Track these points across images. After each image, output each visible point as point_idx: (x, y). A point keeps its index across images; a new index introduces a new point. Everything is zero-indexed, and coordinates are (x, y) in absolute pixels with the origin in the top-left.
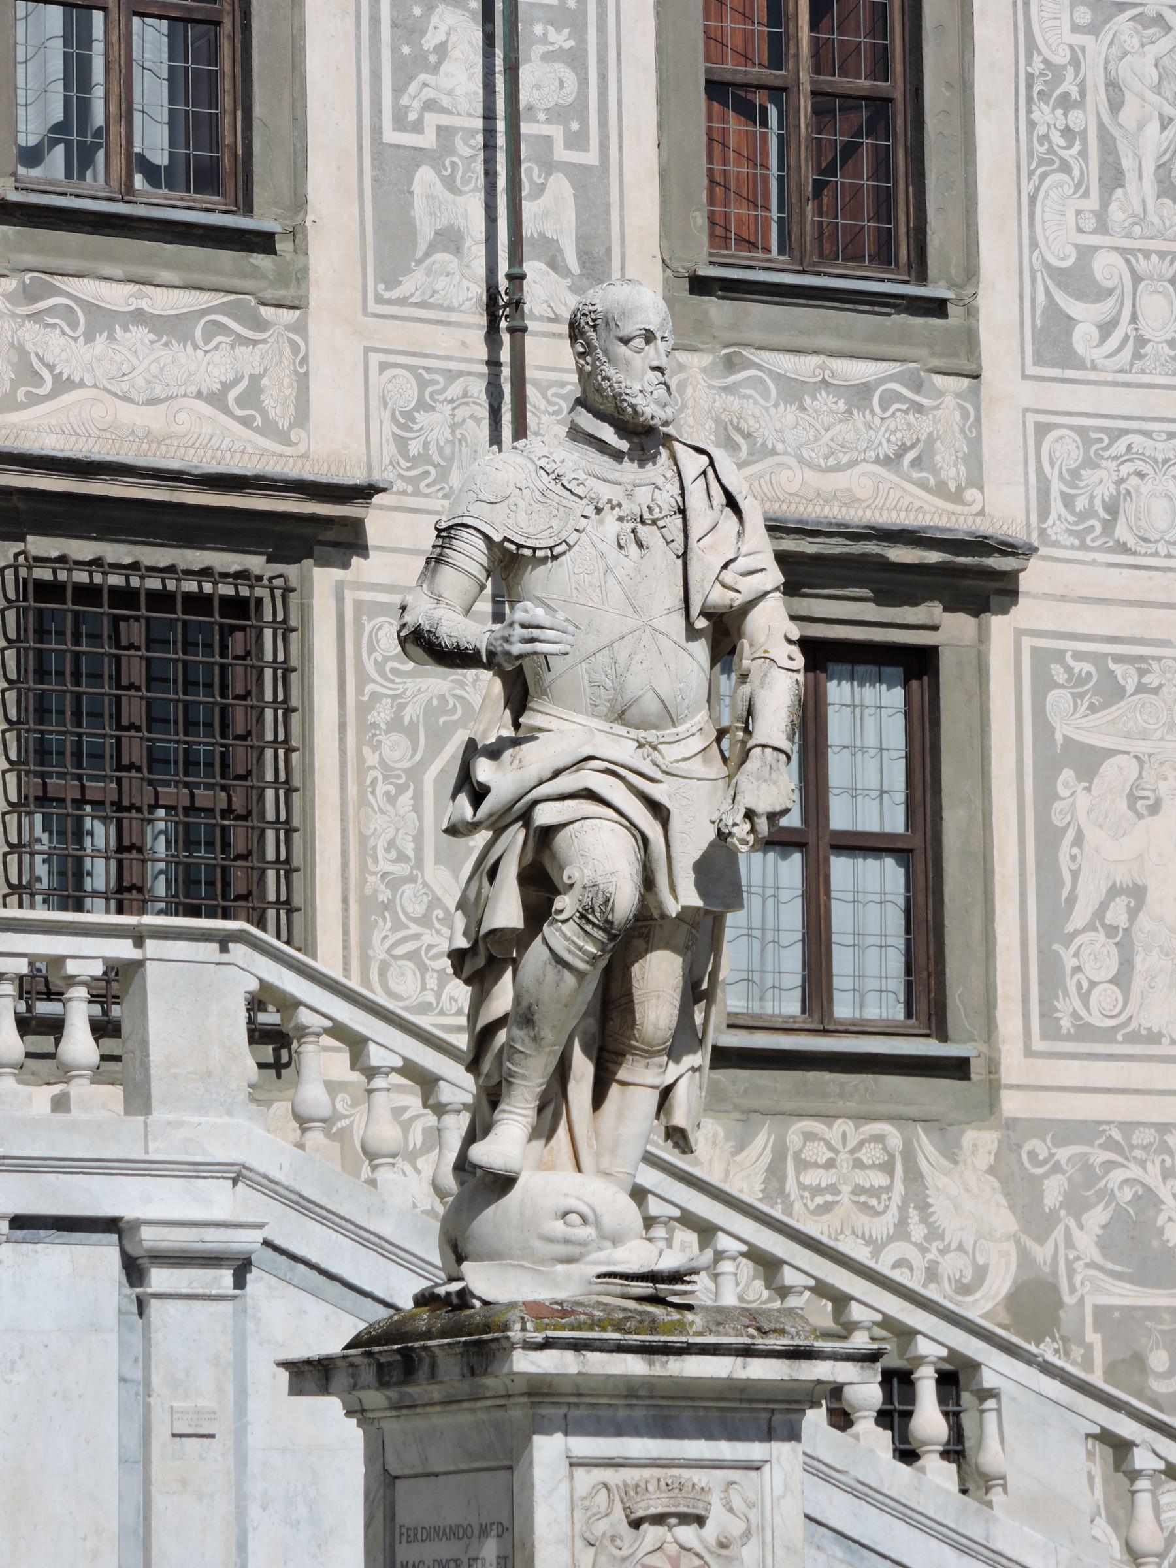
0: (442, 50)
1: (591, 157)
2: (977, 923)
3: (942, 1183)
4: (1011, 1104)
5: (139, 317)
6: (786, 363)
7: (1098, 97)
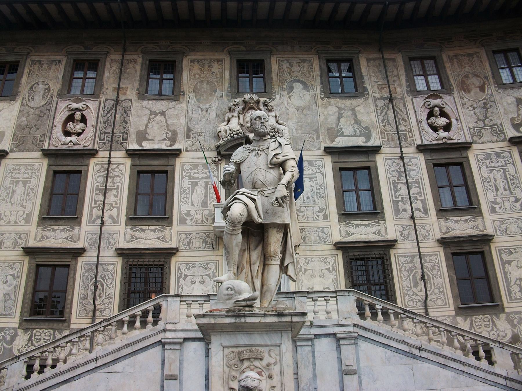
0: (400, 188)
1: (423, 198)
2: (497, 286)
3: (498, 322)
4: (507, 310)
5: (362, 225)
6: (455, 218)
7: (493, 181)
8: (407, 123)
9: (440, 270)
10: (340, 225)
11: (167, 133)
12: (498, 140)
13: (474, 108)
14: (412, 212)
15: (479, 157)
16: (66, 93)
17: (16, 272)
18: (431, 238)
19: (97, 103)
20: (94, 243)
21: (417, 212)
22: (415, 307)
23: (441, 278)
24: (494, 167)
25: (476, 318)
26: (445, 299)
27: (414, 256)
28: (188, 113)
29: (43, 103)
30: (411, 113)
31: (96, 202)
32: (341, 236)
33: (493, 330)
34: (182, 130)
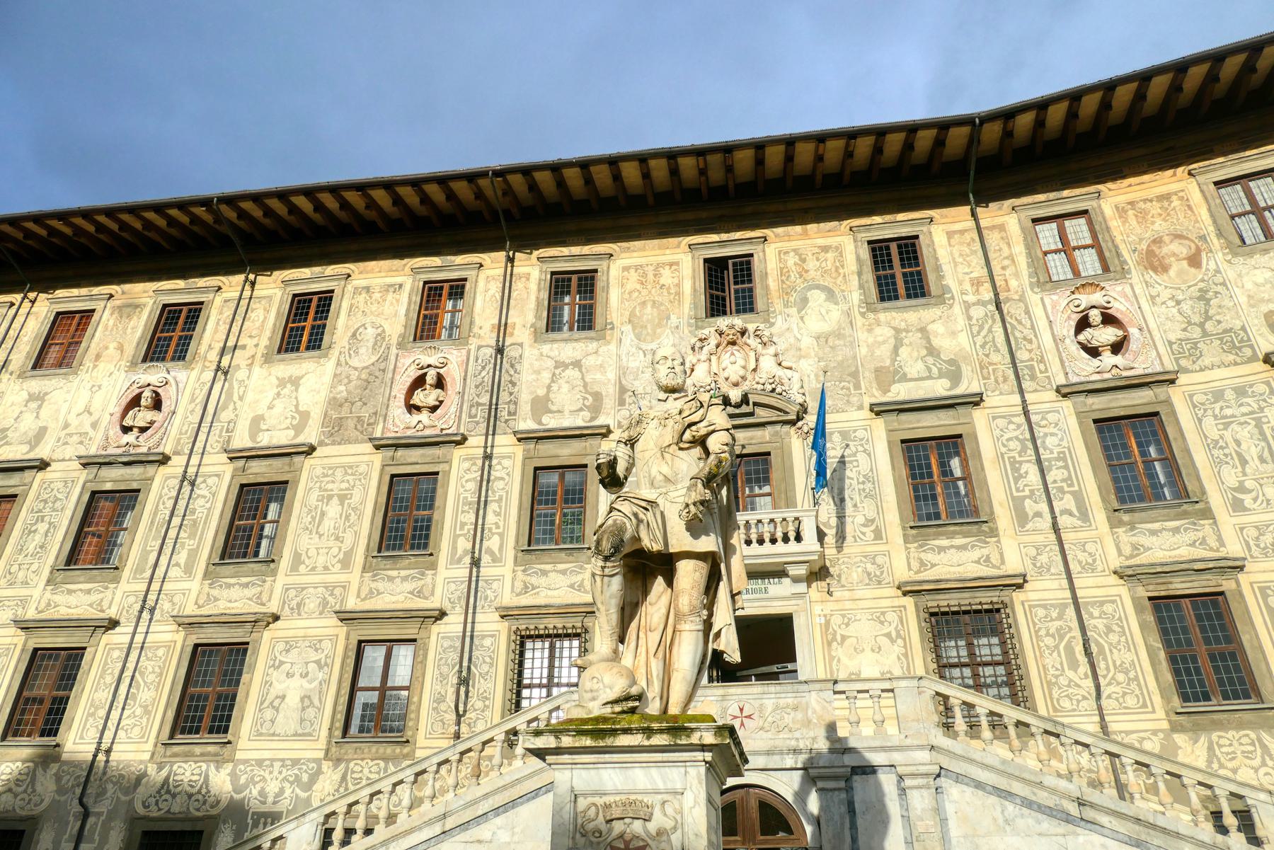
0: (1026, 473)
1: (1076, 488)
5: (952, 547)
7: (1232, 445)
8: (1034, 346)
9: (1124, 633)
10: (907, 548)
11: (585, 398)
12: (1238, 360)
13: (1178, 303)
14: (1054, 518)
15: (1195, 398)
16: (412, 338)
17: (323, 656)
18: (1100, 568)
19: (464, 352)
20: (459, 598)
21: (1065, 517)
22: (1074, 710)
23: (1129, 650)
24: (1233, 416)
25: (1220, 737)
26: (1142, 694)
27: (1066, 606)
28: (621, 360)
29: (374, 358)
30: (1042, 324)
31: (463, 525)
32: (910, 569)
33: (1264, 764)
34: (611, 390)
